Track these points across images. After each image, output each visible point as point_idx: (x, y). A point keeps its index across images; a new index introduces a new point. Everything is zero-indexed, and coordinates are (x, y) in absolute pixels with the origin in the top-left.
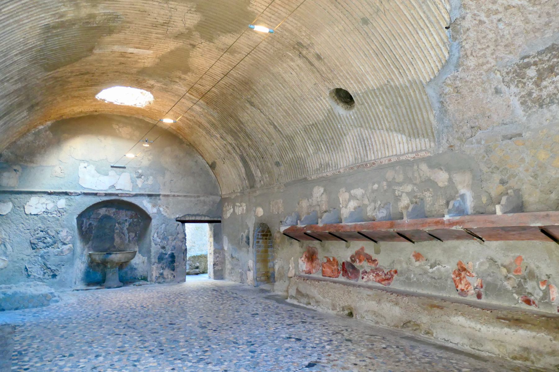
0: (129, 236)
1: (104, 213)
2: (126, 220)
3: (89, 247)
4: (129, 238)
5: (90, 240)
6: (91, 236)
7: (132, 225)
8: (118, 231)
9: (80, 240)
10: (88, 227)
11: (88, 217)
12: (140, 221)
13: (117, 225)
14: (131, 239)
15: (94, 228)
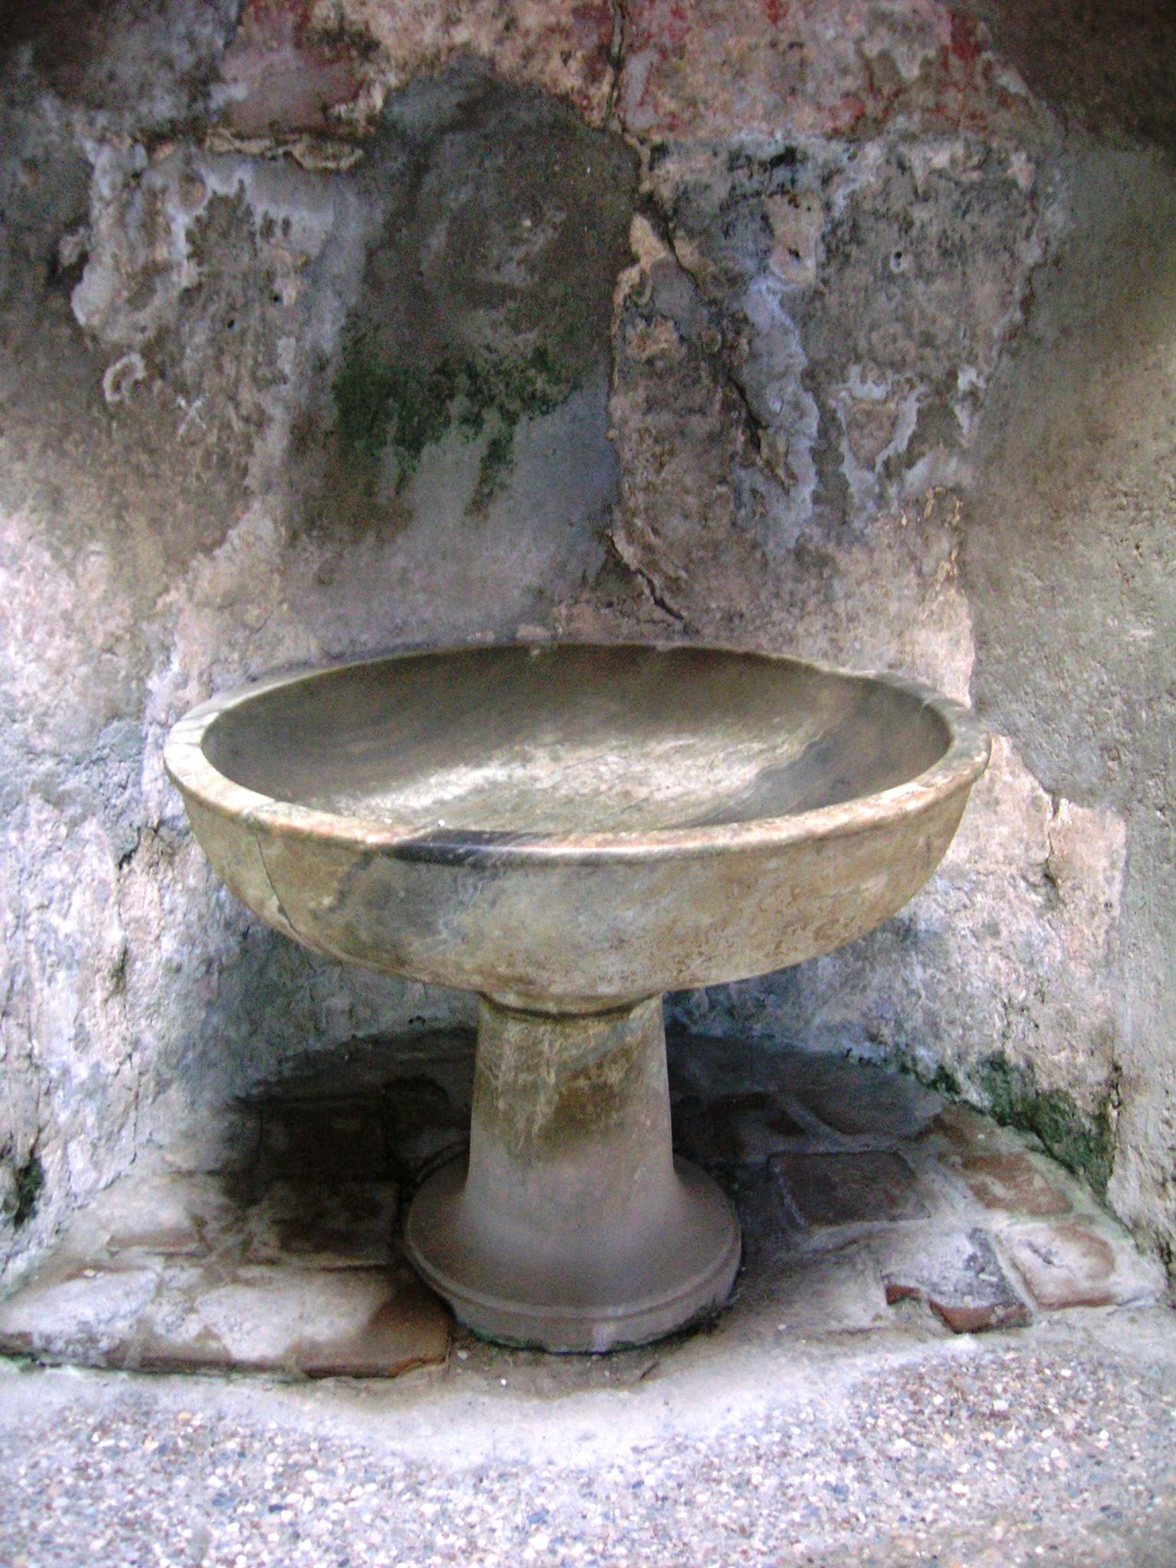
0: (828, 419)
1: (429, 34)
2: (788, 157)
3: (231, 603)
4: (824, 455)
5: (246, 493)
6: (259, 421)
7: (884, 237)
8: (665, 338)
9: (55, 499)
10: (186, 275)
11: (164, 107)
12: (1019, 168)
13: (642, 233)
14: (849, 469)
15: (289, 292)
